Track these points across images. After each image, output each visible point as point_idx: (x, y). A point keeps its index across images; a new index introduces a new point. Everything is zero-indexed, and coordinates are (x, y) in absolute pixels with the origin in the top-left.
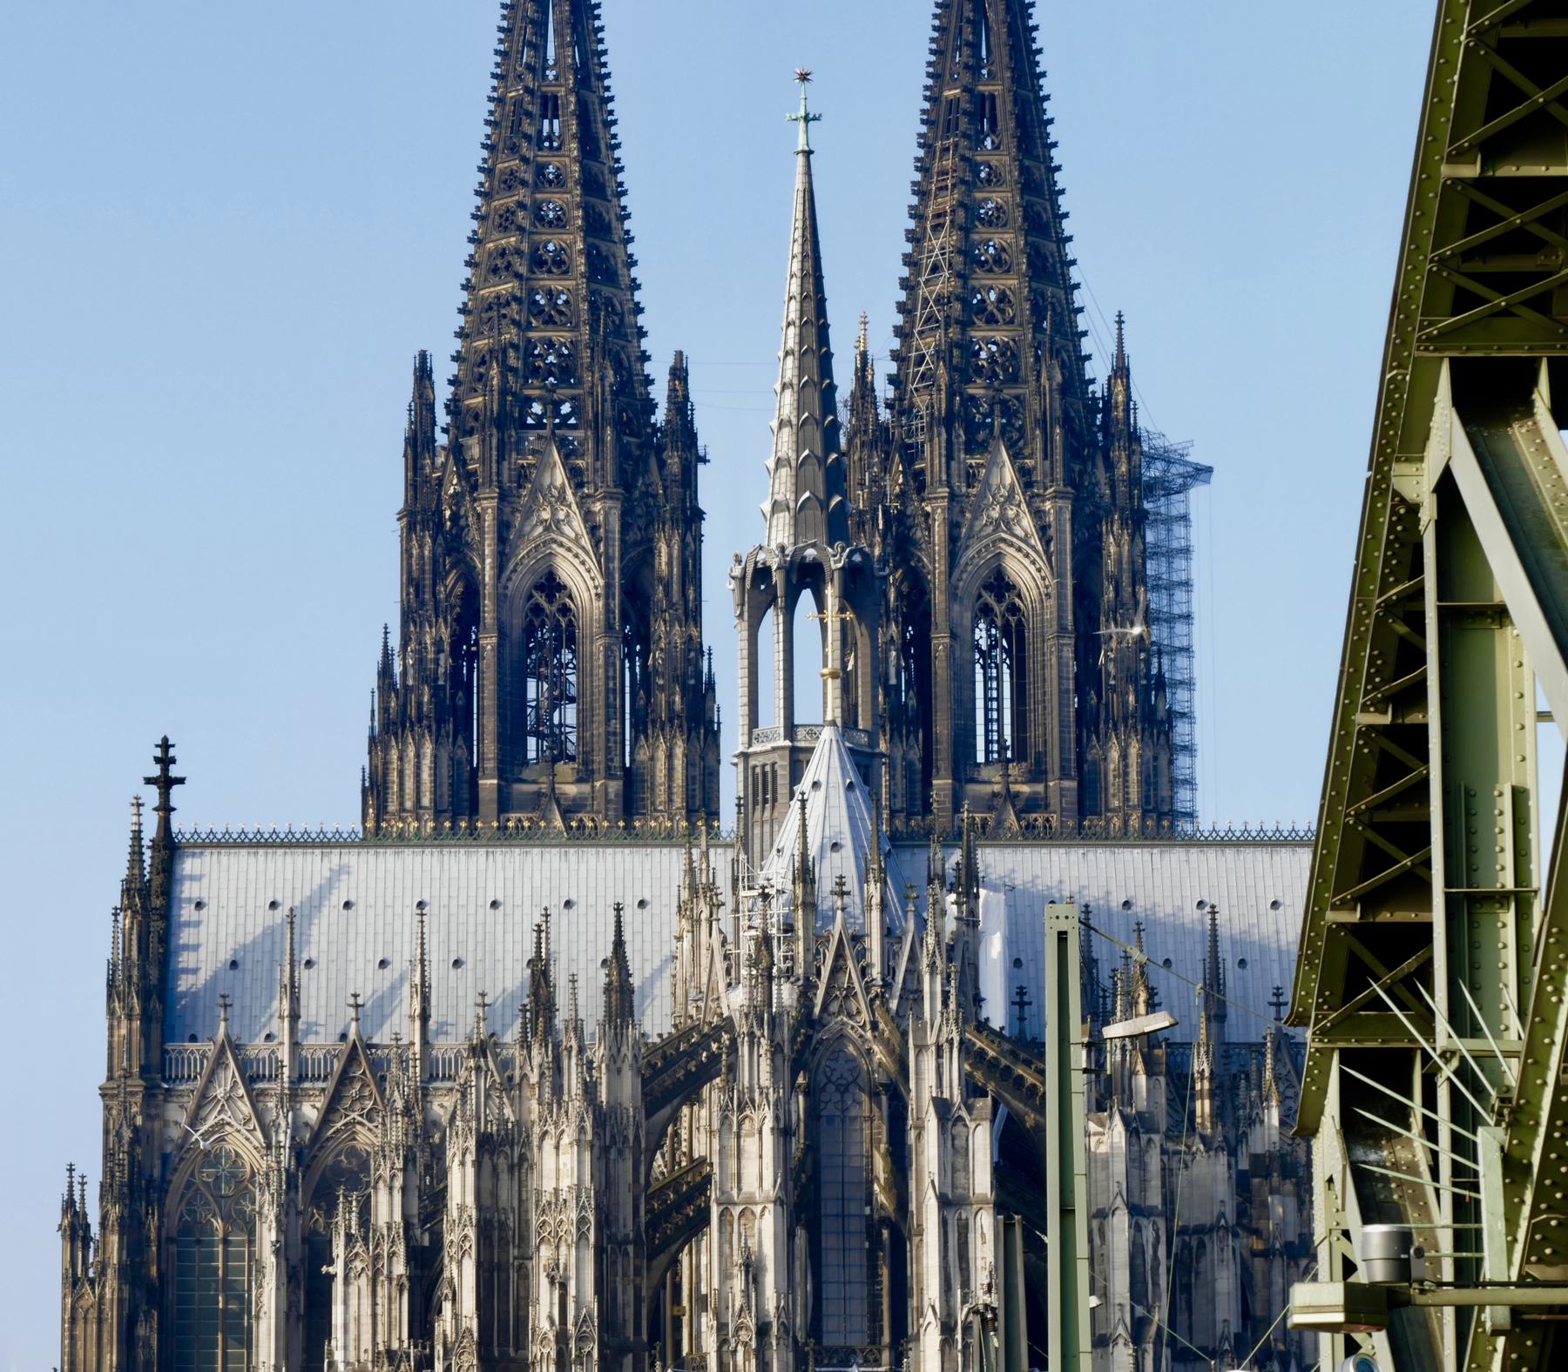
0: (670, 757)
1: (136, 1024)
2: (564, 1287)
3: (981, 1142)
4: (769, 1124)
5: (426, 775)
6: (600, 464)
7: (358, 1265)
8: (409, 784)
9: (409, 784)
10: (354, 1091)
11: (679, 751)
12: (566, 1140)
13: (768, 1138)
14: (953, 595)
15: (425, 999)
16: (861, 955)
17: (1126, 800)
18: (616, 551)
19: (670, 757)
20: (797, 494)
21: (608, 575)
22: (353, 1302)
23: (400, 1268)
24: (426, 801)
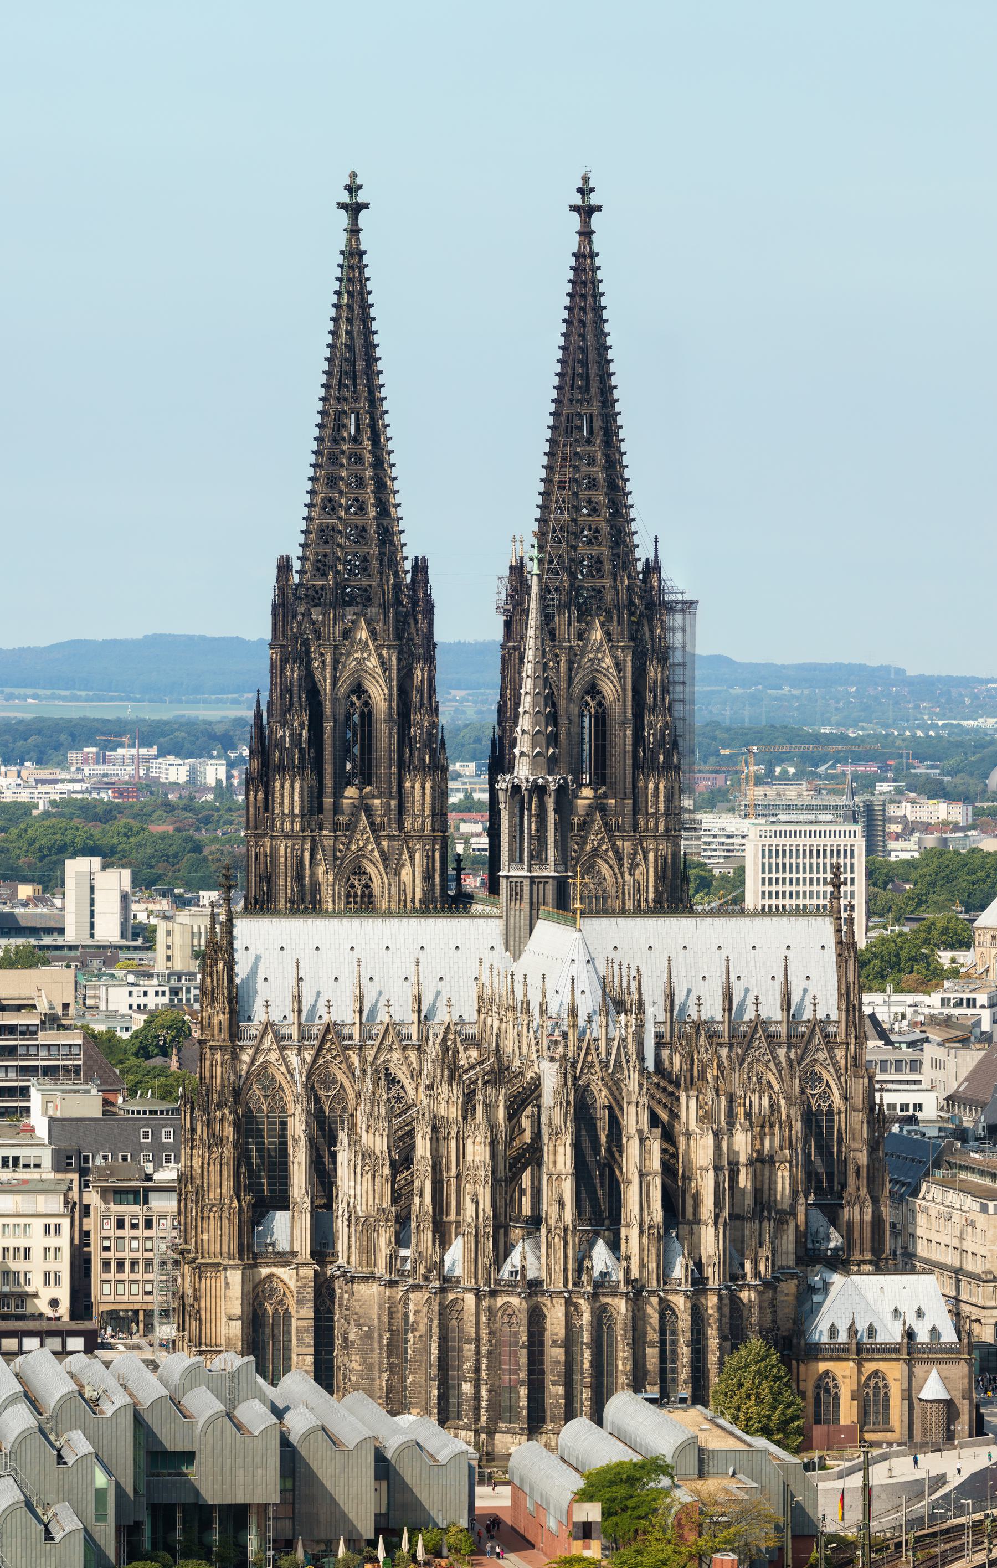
0: (423, 788)
1: (227, 1016)
2: (477, 1203)
3: (655, 1147)
4: (569, 1142)
5: (296, 797)
6: (385, 629)
7: (367, 1168)
8: (287, 800)
9: (287, 800)
10: (328, 1045)
11: (428, 786)
12: (478, 1140)
13: (568, 1148)
14: (569, 699)
15: (361, 1002)
16: (597, 1048)
17: (657, 810)
18: (394, 676)
19: (423, 788)
20: (533, 748)
21: (390, 689)
22: (365, 1184)
23: (387, 1171)
24: (297, 811)
